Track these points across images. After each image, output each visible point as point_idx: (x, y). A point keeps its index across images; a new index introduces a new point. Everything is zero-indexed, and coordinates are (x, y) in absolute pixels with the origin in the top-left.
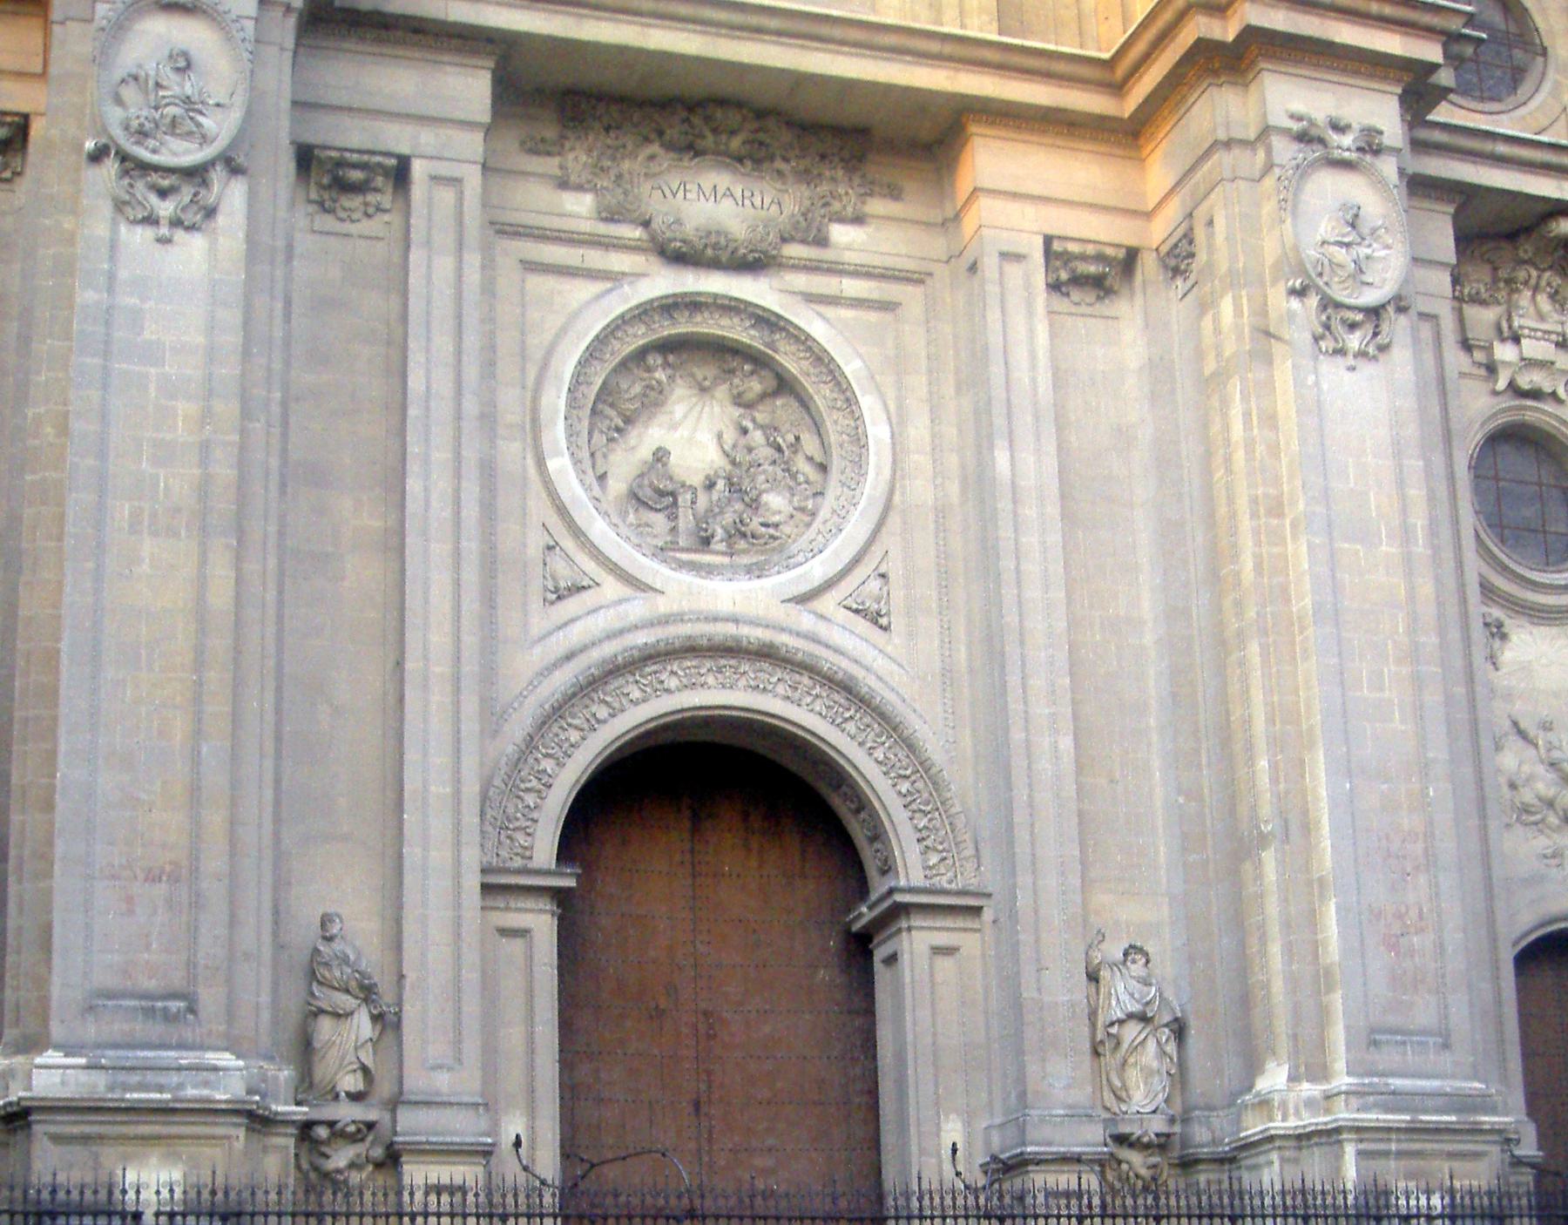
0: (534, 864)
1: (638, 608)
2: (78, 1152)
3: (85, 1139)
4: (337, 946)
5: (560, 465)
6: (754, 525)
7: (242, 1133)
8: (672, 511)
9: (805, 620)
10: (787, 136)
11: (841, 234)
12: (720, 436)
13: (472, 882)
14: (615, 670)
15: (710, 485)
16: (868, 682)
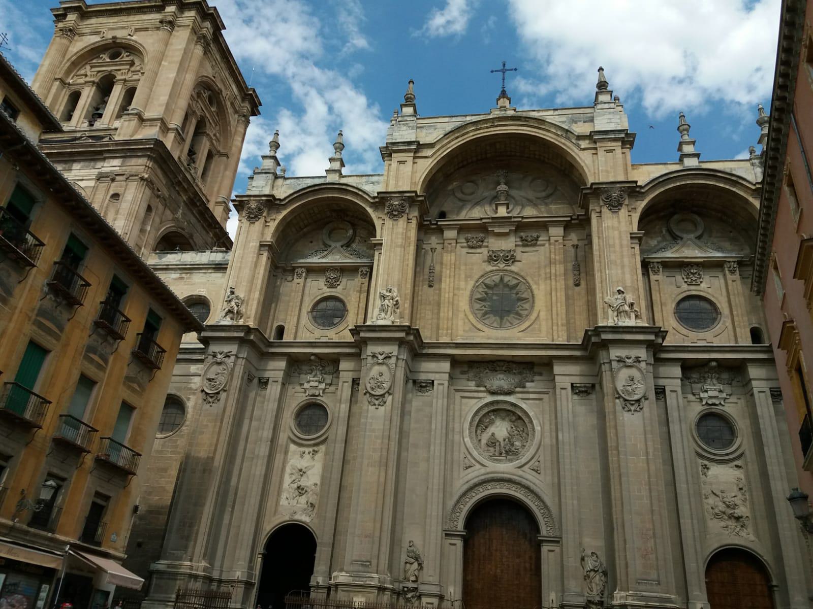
0: (458, 529)
1: (483, 470)
2: (346, 594)
3: (347, 591)
4: (412, 548)
5: (467, 440)
6: (513, 449)
7: (376, 591)
8: (494, 447)
9: (520, 472)
10: (514, 366)
11: (528, 384)
12: (507, 429)
13: (439, 534)
14: (476, 485)
15: (504, 440)
16: (533, 487)
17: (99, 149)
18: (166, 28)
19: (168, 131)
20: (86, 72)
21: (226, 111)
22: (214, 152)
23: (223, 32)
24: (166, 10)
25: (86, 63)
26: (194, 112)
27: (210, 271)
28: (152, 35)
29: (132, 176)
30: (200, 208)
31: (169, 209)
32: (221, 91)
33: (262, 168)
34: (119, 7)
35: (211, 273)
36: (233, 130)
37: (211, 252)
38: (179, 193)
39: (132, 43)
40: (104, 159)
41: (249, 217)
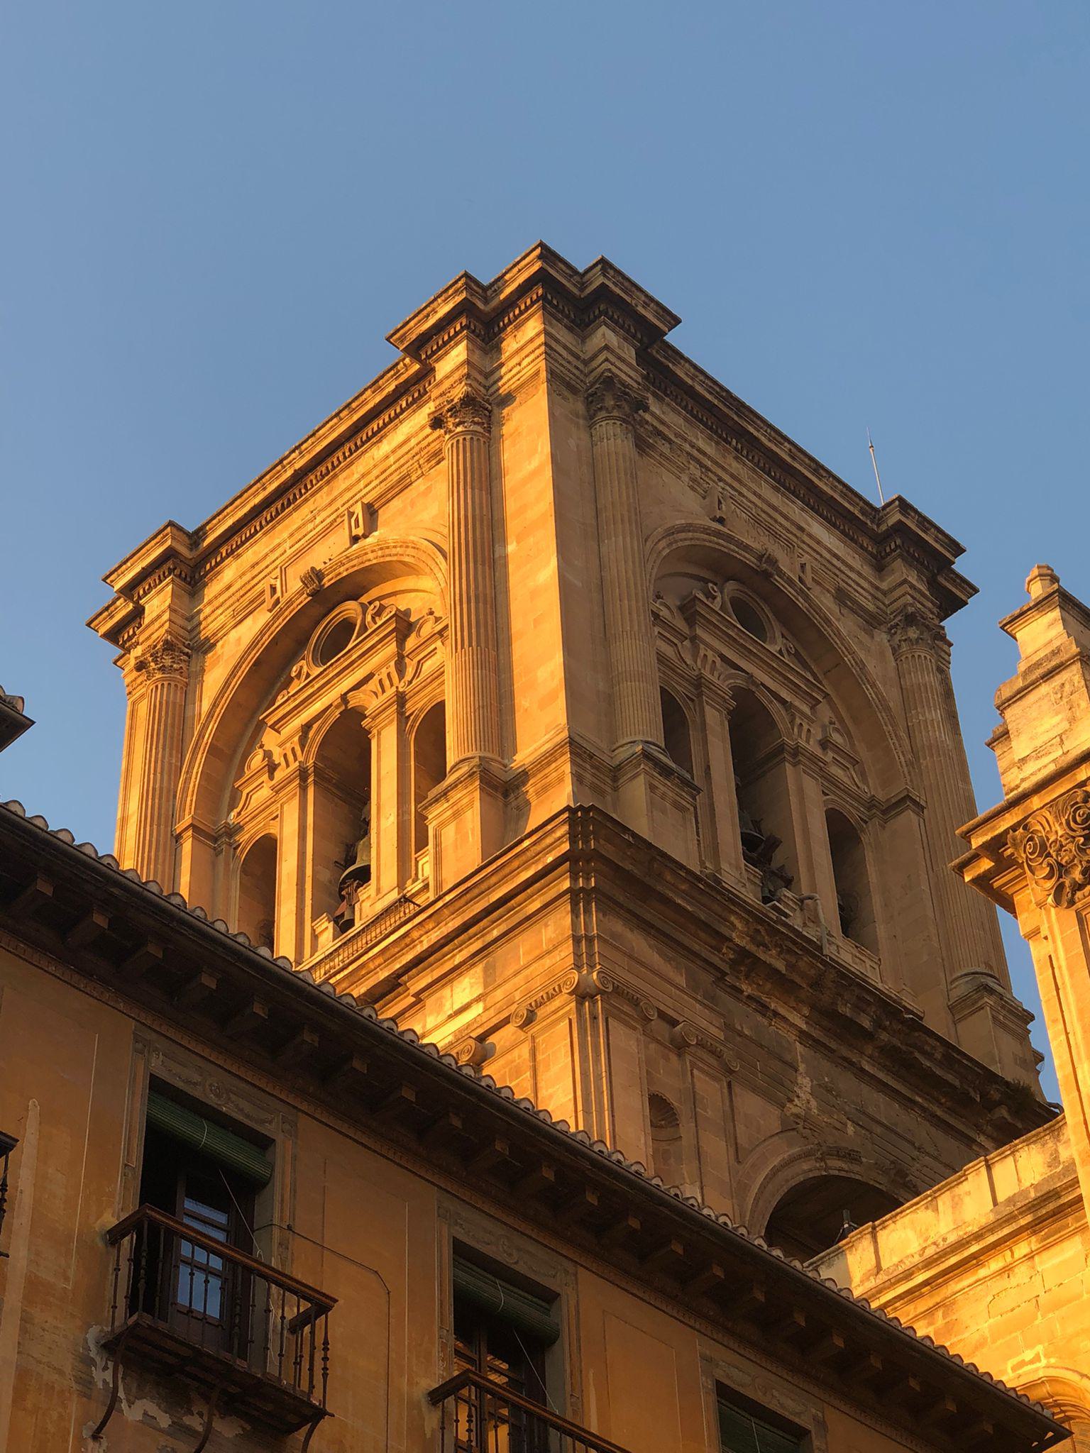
17: (383, 974)
18: (460, 429)
19: (615, 779)
20: (268, 755)
21: (827, 631)
22: (853, 812)
23: (672, 338)
24: (439, 376)
25: (261, 726)
26: (699, 683)
27: (1022, 1249)
28: (429, 489)
29: (540, 1004)
30: (884, 1036)
31: (755, 1090)
32: (772, 561)
33: (1022, 667)
34: (289, 473)
35: (1030, 1257)
36: (893, 697)
37: (989, 1168)
38: (763, 1009)
39: (372, 559)
40: (419, 998)
41: (1059, 889)
